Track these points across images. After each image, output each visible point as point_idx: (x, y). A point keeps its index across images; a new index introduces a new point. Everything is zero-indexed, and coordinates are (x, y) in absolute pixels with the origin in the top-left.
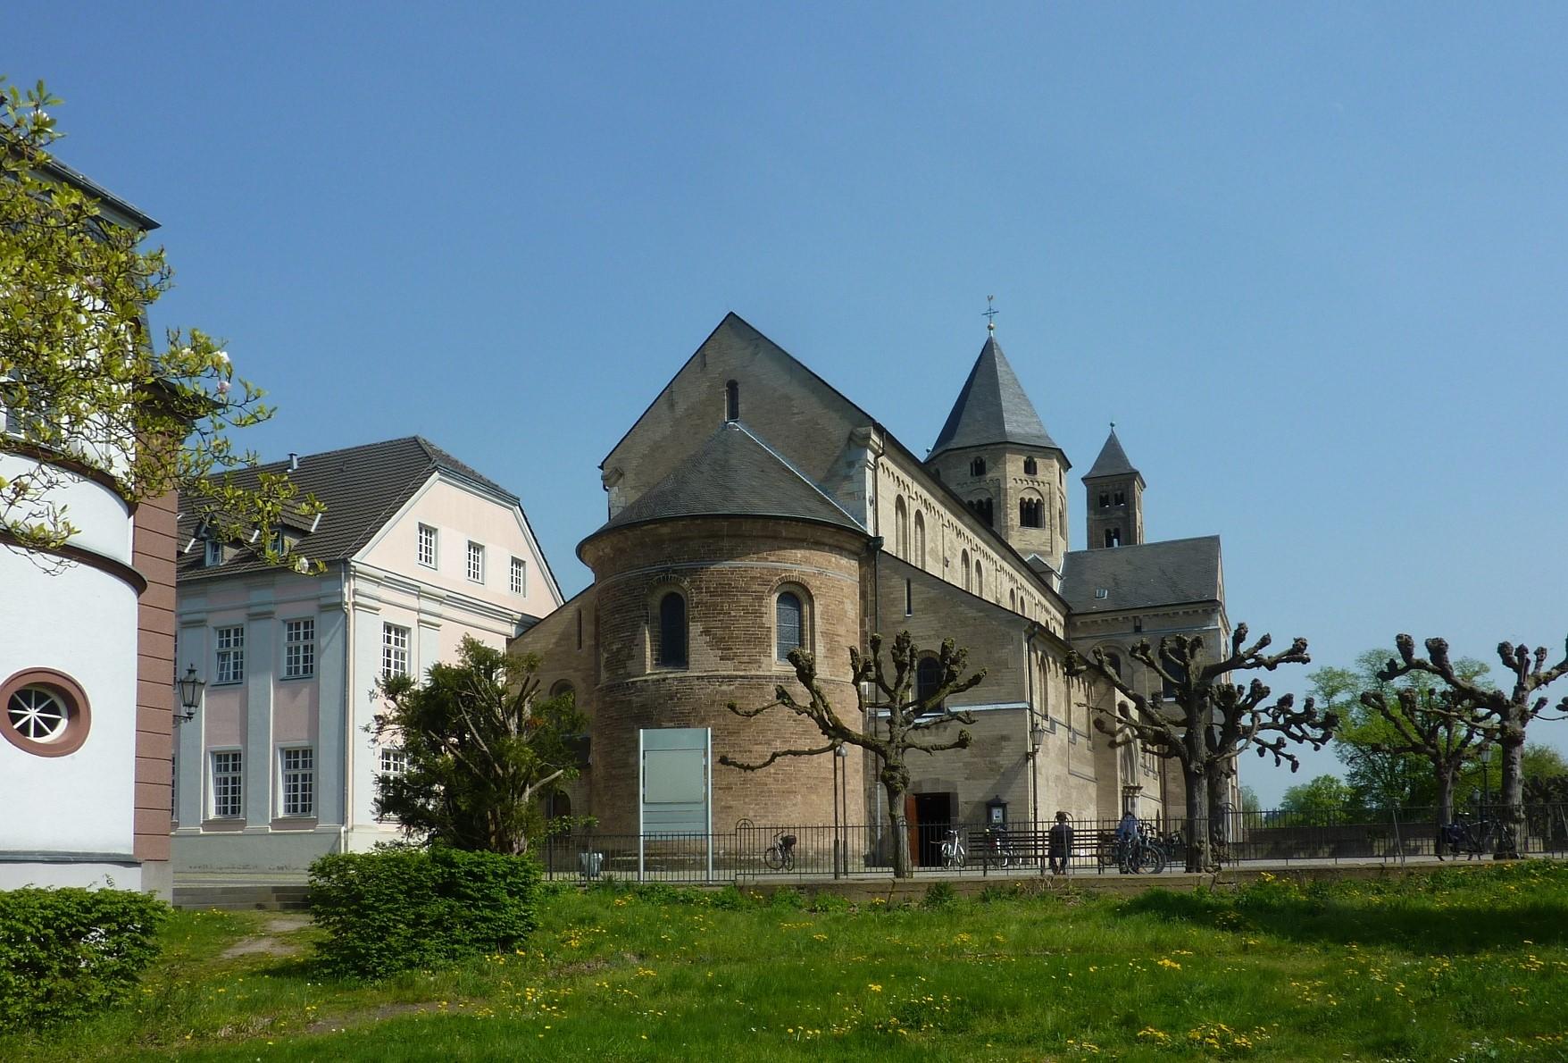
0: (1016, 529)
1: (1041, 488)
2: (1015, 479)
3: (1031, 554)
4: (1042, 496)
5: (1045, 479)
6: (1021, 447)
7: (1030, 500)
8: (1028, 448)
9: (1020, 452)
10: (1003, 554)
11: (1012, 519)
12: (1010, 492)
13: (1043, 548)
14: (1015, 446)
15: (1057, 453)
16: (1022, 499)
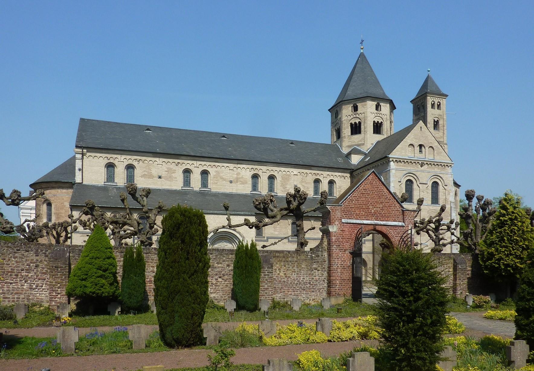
0: (347, 137)
1: (360, 116)
2: (346, 116)
3: (353, 146)
4: (360, 120)
5: (362, 112)
6: (350, 101)
7: (355, 123)
8: (353, 100)
9: (349, 103)
10: (237, 163)
11: (344, 134)
12: (344, 122)
13: (360, 143)
14: (346, 102)
15: (369, 98)
16: (351, 124)
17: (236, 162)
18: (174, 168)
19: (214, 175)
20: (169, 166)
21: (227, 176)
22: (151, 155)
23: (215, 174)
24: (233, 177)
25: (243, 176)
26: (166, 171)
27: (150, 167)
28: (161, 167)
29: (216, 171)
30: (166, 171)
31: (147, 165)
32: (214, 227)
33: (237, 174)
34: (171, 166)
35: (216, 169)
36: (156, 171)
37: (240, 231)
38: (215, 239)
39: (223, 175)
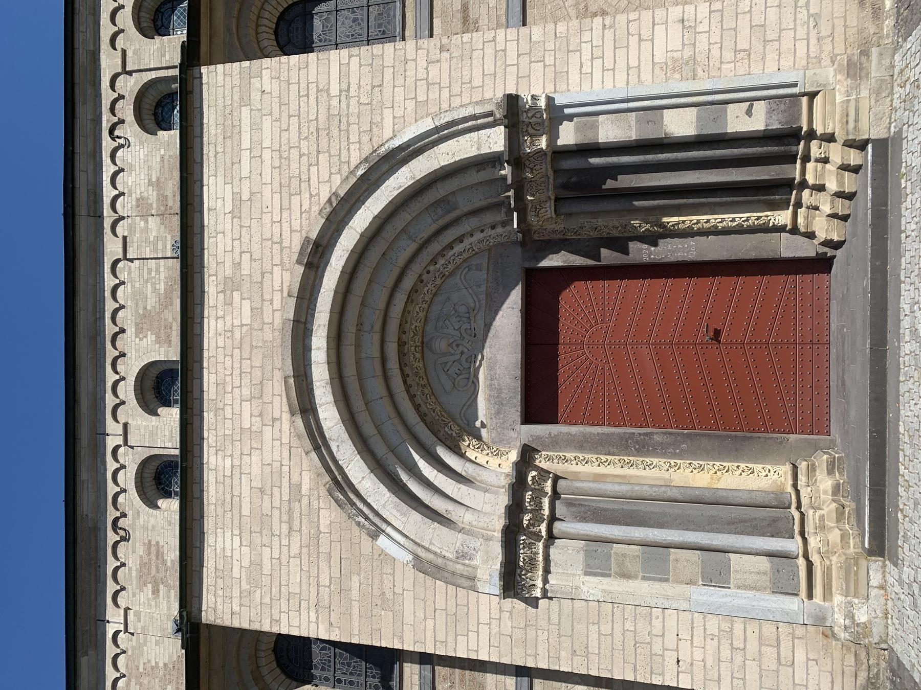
17: (83, 225)
18: (141, 551)
19: (158, 341)
20: (134, 574)
21: (158, 271)
22: (84, 663)
23: (151, 338)
24: (157, 238)
25: (150, 183)
26: (156, 591)
27: (141, 670)
28: (138, 614)
29: (139, 331)
30: (156, 591)
31: (133, 683)
32: (295, 442)
33: (144, 217)
34: (130, 563)
35: (131, 331)
36: (157, 643)
37: (325, 196)
38: (412, 417)
39: (155, 290)
